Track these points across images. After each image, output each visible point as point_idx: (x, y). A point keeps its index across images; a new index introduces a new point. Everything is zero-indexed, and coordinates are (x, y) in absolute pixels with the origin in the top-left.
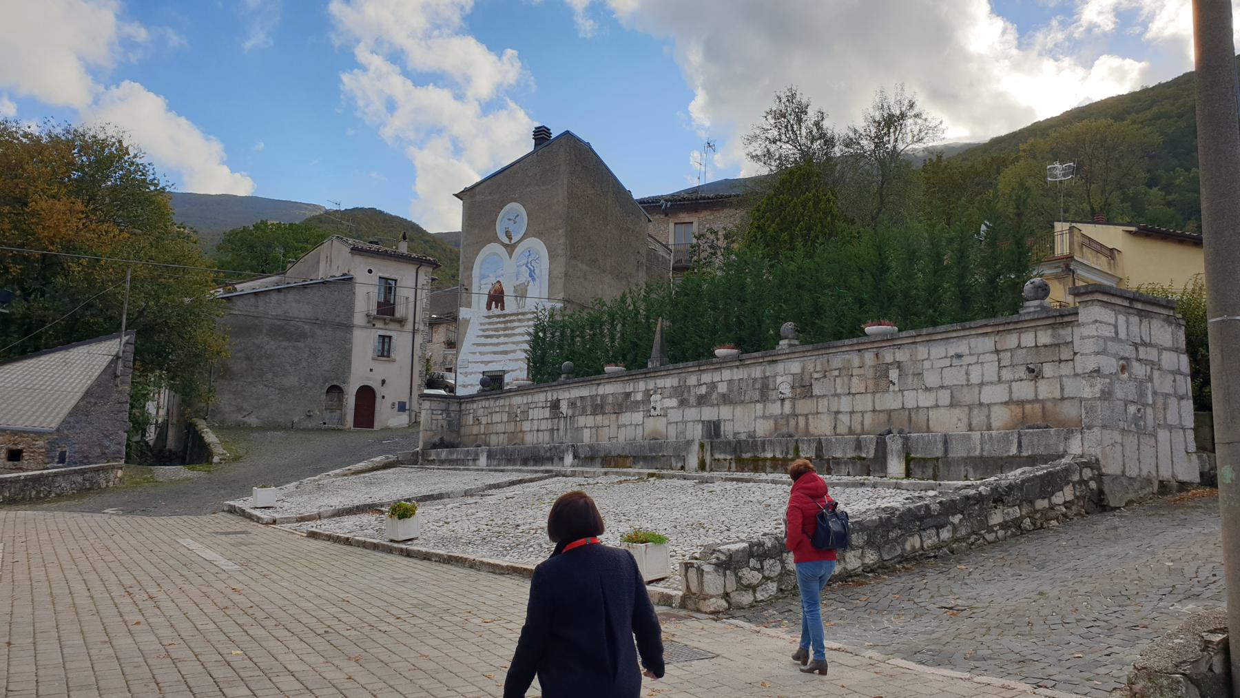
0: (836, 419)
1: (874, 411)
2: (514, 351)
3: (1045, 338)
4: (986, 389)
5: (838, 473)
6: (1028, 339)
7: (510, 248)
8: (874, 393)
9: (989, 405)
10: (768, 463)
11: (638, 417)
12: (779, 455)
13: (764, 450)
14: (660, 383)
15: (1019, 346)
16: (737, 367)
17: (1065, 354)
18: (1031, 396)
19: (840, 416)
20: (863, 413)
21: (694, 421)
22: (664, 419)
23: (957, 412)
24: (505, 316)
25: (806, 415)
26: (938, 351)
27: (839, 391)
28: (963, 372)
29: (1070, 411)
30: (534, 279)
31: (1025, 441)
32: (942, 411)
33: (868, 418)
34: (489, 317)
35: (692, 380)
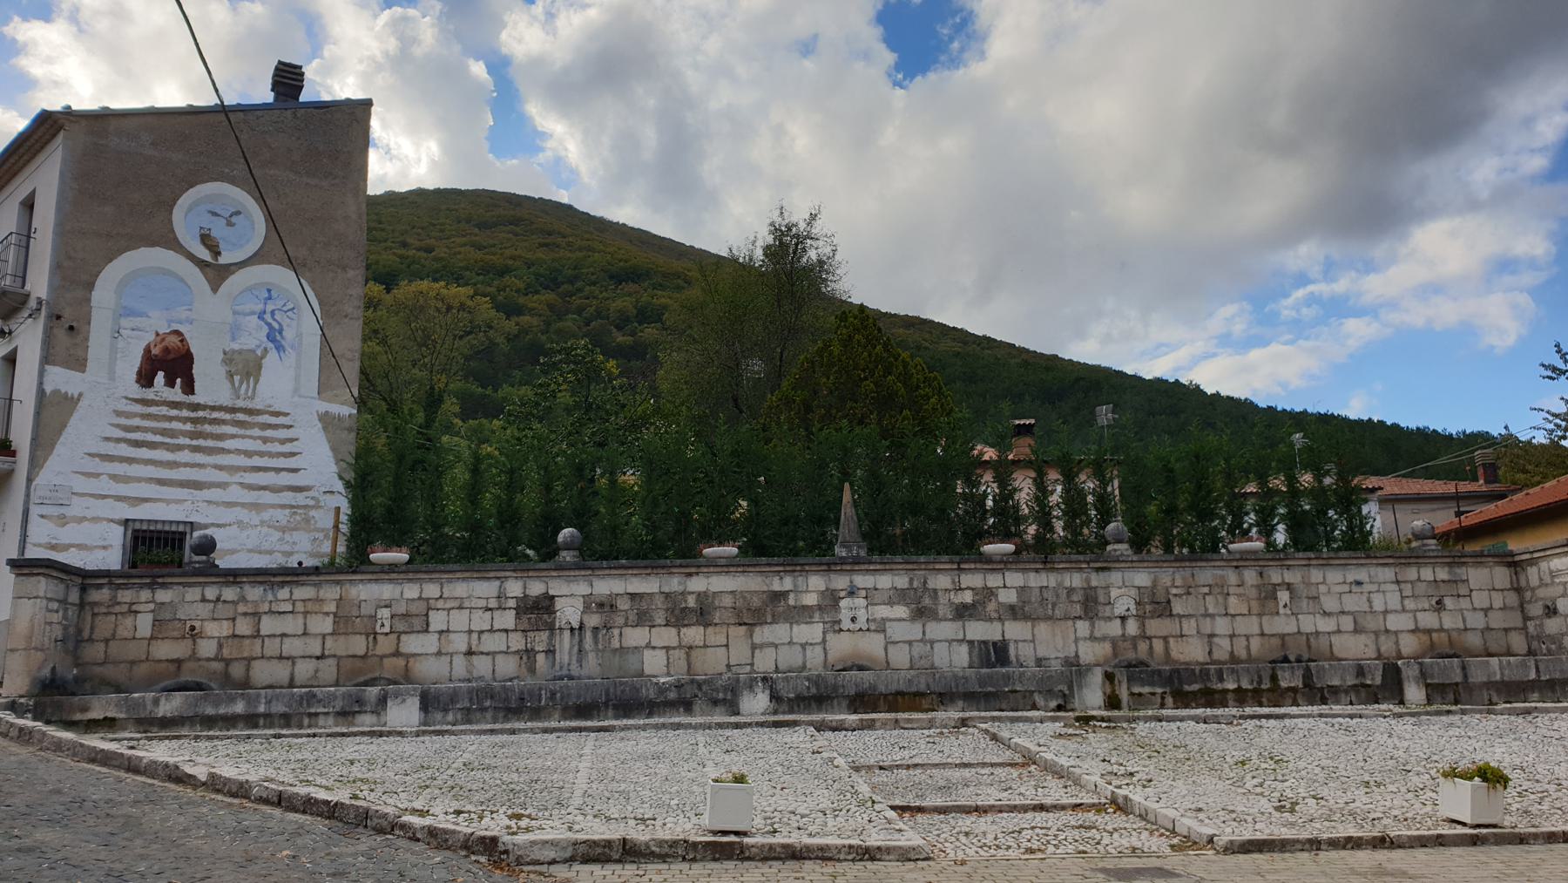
0: (1210, 644)
1: (1262, 635)
3: (1443, 574)
4: (1390, 617)
5: (1337, 702)
6: (1427, 573)
7: (217, 273)
8: (1260, 615)
9: (1396, 633)
10: (1230, 696)
11: (811, 632)
12: (1245, 685)
13: (1221, 679)
15: (1419, 579)
16: (1037, 571)
17: (1463, 590)
18: (1436, 626)
19: (1216, 640)
20: (1247, 637)
21: (950, 642)
23: (1363, 639)
24: (196, 407)
25: (1165, 639)
26: (1334, 576)
27: (1211, 611)
28: (1364, 598)
29: (1474, 640)
30: (280, 348)
31: (1542, 667)
32: (1346, 636)
33: (1255, 644)
35: (941, 581)
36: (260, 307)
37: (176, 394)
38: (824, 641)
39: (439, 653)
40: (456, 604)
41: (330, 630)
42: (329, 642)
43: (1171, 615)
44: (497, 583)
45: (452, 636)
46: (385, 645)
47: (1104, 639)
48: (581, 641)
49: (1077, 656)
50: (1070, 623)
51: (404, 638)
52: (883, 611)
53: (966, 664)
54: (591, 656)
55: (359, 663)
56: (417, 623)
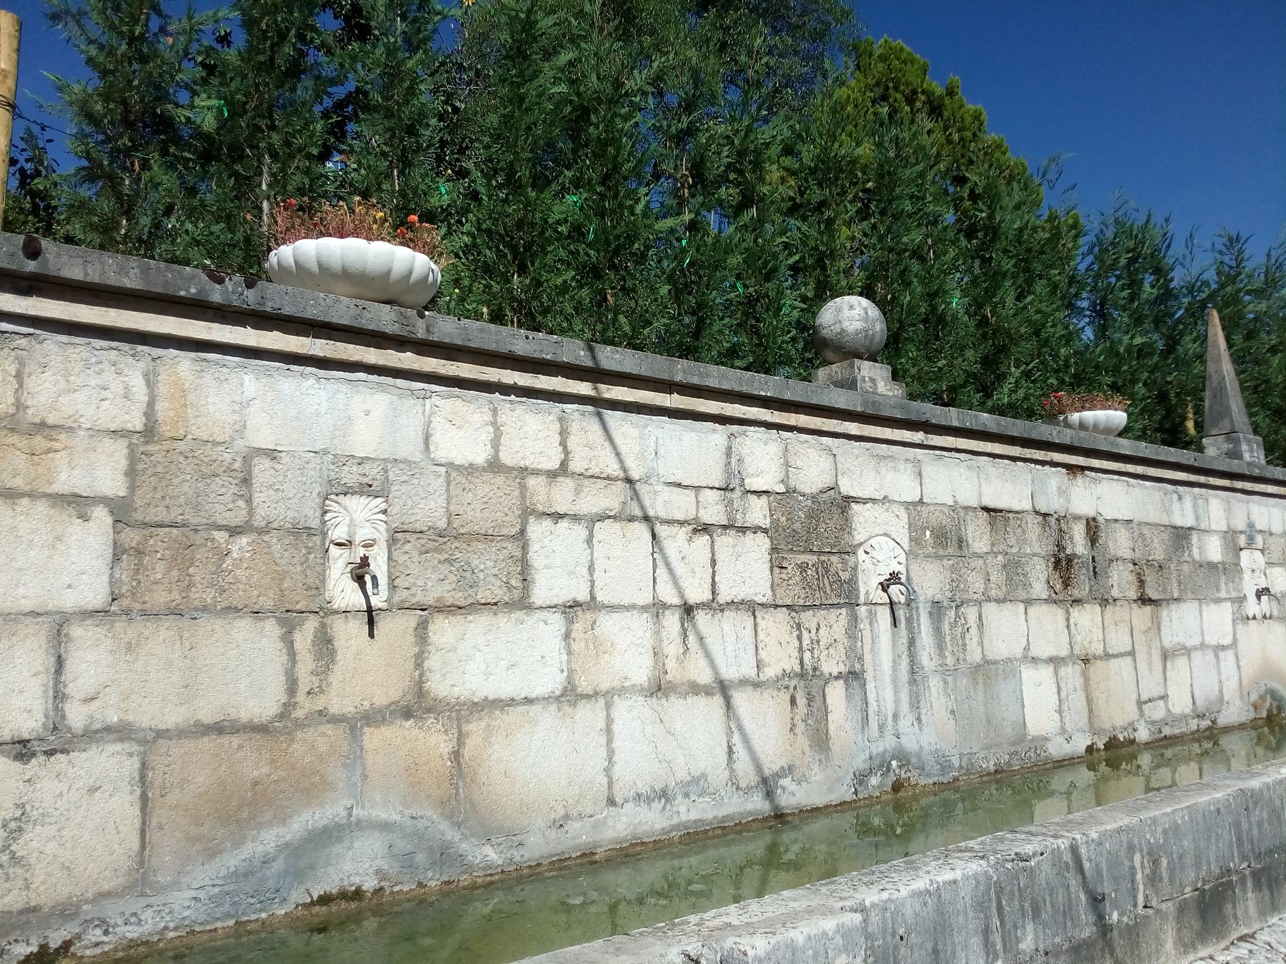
39: (570, 695)
40: (611, 499)
41: (94, 593)
42: (91, 659)
44: (717, 436)
45: (608, 624)
46: (366, 669)
48: (912, 642)
51: (443, 630)
54: (935, 683)
55: (252, 763)
56: (489, 565)
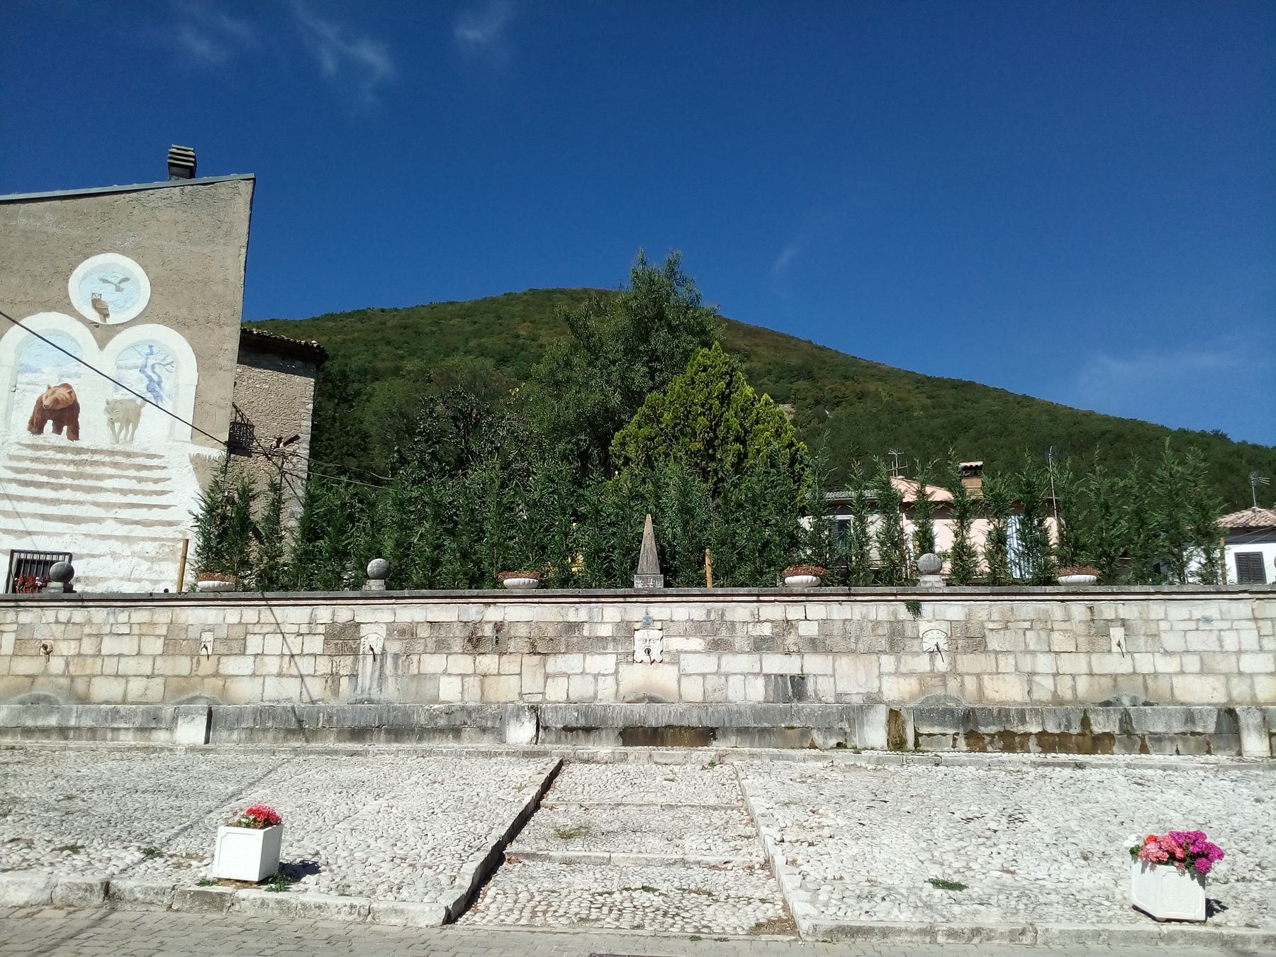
0: (1030, 682)
1: (1091, 674)
2: (99, 520)
7: (104, 333)
9: (1251, 675)
11: (603, 662)
12: (1052, 729)
13: (1023, 721)
14: (659, 611)
19: (1037, 678)
20: (1073, 676)
21: (745, 675)
22: (673, 670)
23: (1210, 681)
24: (79, 451)
27: (1032, 647)
28: (1214, 636)
32: (1189, 679)
34: (35, 447)
35: (740, 612)
36: (141, 362)
37: (63, 439)
38: (617, 672)
39: (254, 675)
40: (271, 629)
41: (160, 652)
42: (159, 662)
43: (985, 651)
44: (309, 609)
45: (266, 659)
46: (207, 666)
47: (911, 674)
48: (382, 667)
49: (880, 691)
50: (874, 657)
51: (223, 660)
52: (676, 643)
53: (762, 699)
55: (183, 683)
56: (236, 646)
